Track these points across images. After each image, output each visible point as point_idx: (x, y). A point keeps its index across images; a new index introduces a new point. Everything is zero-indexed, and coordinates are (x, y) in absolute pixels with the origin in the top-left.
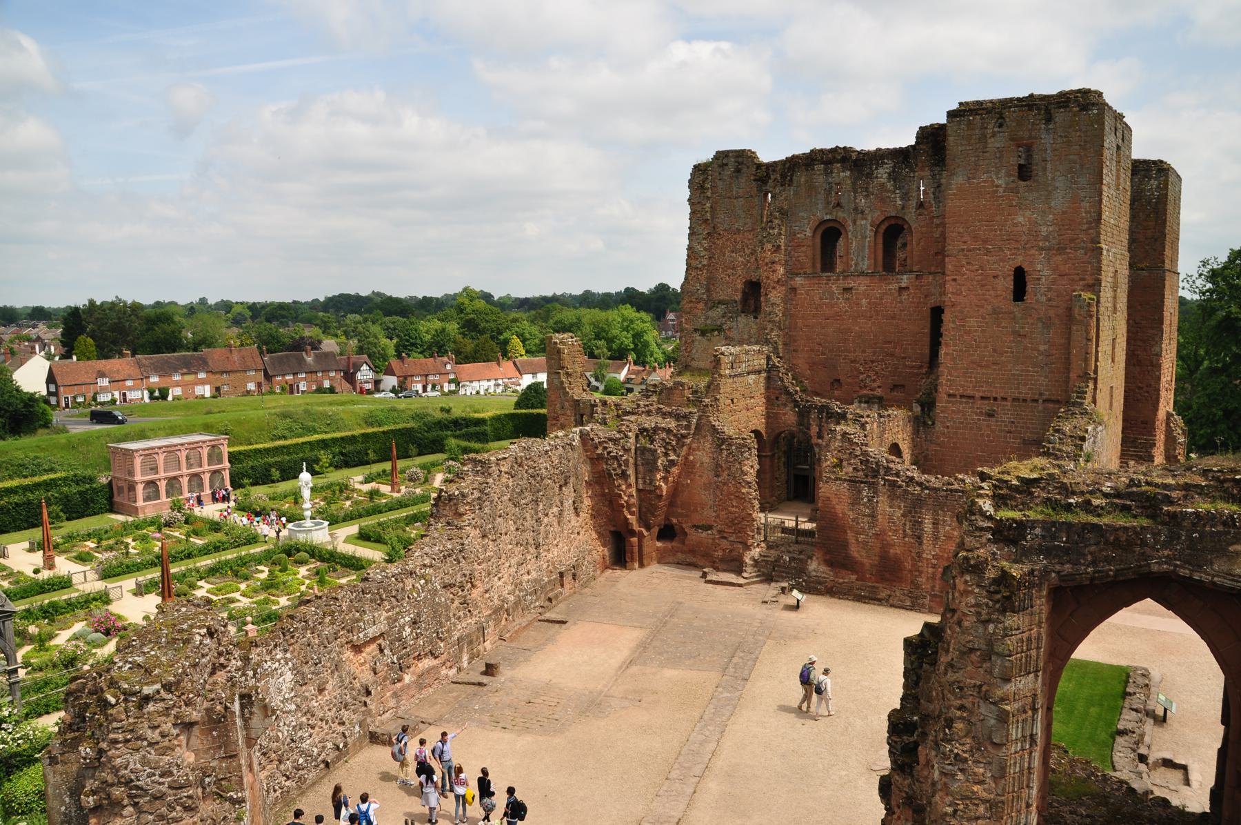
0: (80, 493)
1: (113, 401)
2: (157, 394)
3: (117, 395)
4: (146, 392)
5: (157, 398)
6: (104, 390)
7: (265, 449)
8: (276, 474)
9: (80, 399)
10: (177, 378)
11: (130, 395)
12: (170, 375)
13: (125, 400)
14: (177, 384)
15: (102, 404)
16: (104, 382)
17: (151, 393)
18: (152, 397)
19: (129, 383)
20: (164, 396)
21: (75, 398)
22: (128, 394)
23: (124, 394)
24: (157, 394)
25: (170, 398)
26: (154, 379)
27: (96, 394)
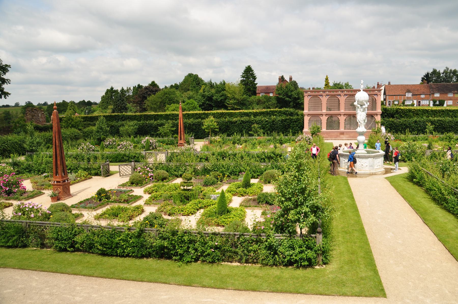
0: (282, 121)
1: (413, 105)
2: (438, 103)
3: (415, 102)
4: (432, 103)
5: (438, 105)
6: (409, 99)
7: (432, 111)
8: (430, 127)
9: (396, 103)
10: (450, 95)
11: (423, 102)
12: (447, 93)
13: (419, 105)
14: (450, 99)
15: (407, 106)
16: (409, 95)
17: (434, 102)
18: (434, 105)
19: (423, 96)
20: (442, 104)
21: (393, 102)
22: (421, 102)
23: (419, 102)
24: (438, 103)
25: (445, 105)
26: (437, 95)
27: (404, 101)
